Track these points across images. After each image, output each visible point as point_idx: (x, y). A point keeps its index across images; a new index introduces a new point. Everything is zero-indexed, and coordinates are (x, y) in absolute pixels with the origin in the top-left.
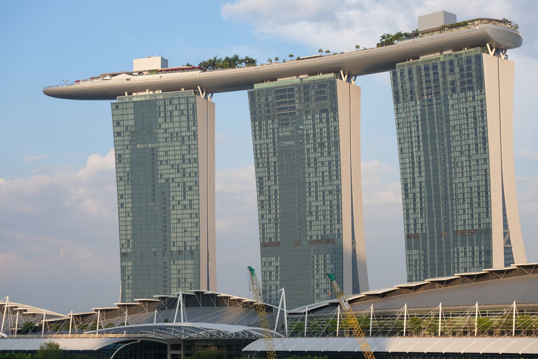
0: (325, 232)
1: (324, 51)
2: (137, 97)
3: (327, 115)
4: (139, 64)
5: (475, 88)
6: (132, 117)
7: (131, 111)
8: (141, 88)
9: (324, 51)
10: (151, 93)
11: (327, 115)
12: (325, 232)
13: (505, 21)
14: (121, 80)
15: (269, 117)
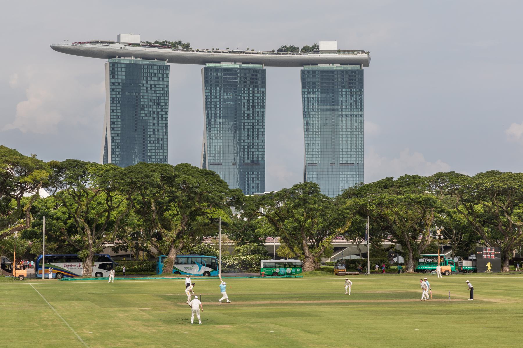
0: (253, 158)
1: (250, 50)
2: (123, 60)
3: (258, 89)
4: (126, 38)
5: (357, 87)
6: (124, 73)
7: (124, 69)
8: (129, 55)
9: (250, 50)
10: (134, 59)
11: (258, 89)
12: (253, 158)
13: (368, 53)
14: (115, 47)
15: (218, 86)
